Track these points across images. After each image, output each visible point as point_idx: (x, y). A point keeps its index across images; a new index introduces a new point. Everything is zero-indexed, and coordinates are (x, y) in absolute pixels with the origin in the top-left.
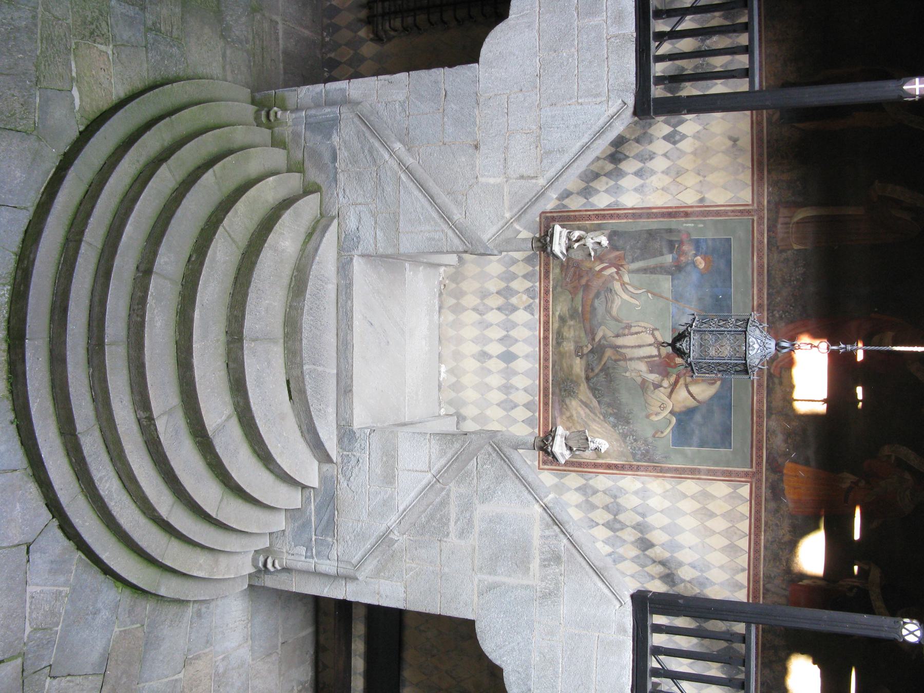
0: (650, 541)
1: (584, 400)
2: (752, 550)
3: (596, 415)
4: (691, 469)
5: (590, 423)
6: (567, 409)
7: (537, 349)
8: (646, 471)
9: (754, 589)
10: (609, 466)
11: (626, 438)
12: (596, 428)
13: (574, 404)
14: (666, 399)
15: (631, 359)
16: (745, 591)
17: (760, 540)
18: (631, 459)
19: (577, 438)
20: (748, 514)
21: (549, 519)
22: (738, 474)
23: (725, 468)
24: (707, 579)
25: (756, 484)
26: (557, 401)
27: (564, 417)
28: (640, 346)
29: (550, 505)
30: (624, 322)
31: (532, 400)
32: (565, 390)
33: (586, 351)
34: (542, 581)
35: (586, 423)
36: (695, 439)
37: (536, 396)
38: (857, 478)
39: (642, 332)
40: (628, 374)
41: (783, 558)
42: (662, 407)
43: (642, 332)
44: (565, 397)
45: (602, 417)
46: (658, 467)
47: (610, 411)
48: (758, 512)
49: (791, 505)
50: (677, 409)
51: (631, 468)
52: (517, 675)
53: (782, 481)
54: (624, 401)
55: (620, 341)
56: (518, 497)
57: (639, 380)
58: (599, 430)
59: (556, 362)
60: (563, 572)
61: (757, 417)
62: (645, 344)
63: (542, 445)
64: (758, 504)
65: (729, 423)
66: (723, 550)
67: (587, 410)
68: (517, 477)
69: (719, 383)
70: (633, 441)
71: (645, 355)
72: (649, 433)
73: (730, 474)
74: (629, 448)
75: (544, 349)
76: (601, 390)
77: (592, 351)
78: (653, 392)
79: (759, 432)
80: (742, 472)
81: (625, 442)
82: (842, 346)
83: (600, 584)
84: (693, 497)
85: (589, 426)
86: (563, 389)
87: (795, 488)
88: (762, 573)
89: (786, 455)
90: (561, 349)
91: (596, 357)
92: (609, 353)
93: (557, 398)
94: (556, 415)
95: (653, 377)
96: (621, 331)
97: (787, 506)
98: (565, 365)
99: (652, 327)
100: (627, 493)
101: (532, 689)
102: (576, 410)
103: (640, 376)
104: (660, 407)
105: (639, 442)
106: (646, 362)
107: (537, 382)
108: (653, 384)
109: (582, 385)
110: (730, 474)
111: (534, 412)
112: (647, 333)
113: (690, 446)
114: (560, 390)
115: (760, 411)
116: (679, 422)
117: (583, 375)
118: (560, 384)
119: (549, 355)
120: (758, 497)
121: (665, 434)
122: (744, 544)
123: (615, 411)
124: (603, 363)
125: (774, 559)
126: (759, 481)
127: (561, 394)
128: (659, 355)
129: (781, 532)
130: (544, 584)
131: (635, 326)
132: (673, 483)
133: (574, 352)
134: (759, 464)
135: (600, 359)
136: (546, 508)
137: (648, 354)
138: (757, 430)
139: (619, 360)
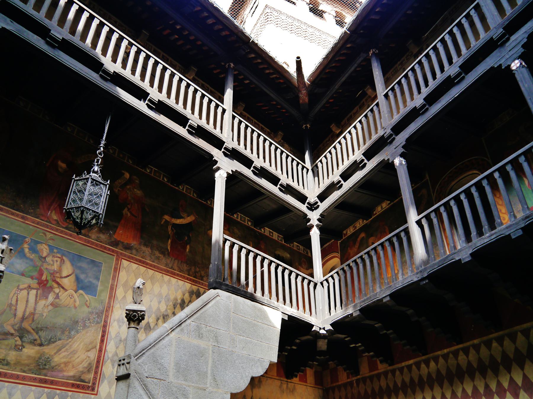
0: (146, 324)
1: (55, 351)
2: (154, 269)
3: (68, 344)
4: (110, 289)
5: (72, 350)
6: (59, 365)
7: (7, 384)
8: (108, 316)
9: (171, 274)
10: (102, 341)
11: (86, 326)
12: (76, 346)
13: (57, 359)
14: (67, 293)
15: (35, 309)
16: (172, 278)
17: (149, 263)
18: (100, 325)
19: (137, 295)
20: (137, 265)
21: (178, 329)
22: (117, 264)
23: (113, 269)
24: (166, 296)
25: (123, 256)
26: (52, 373)
27: (64, 369)
28: (27, 301)
29: (171, 327)
30: (5, 307)
31: (47, 394)
32: (45, 365)
33: (19, 342)
34: (209, 341)
35: (71, 352)
36: (94, 281)
37: (44, 390)
38: (126, 208)
39: (17, 296)
40: (45, 315)
41: (159, 255)
42: (71, 296)
43: (17, 296)
44: (50, 365)
45: (70, 340)
46: (106, 309)
47: (67, 333)
48: (136, 260)
49: (135, 243)
50: (75, 288)
51: (105, 326)
52: (253, 367)
53: (123, 243)
54: (62, 322)
55: (20, 314)
56: (166, 347)
57: (50, 308)
58: (78, 343)
59: (21, 369)
60: (205, 326)
61: (88, 243)
62: (26, 297)
63: (137, 322)
64: (133, 258)
65: (88, 260)
66: (153, 284)
67: (63, 350)
68: (154, 346)
69: (64, 258)
70: (89, 321)
71: (34, 299)
72: (86, 310)
73: (116, 269)
74: (93, 325)
75: (8, 378)
76: (51, 337)
77: (21, 338)
78: (61, 300)
79: (97, 245)
80: (116, 261)
81: (89, 327)
82: (102, 145)
83: (210, 305)
84: (126, 293)
85: (74, 351)
86: (44, 366)
87: (127, 238)
88: (164, 268)
89: (110, 236)
90: (12, 362)
91: (27, 335)
92: (26, 325)
93: (50, 373)
94: (61, 375)
95: (51, 297)
96: (12, 312)
97: (135, 245)
98: (26, 362)
99: (15, 289)
100: (119, 332)
101: (259, 358)
102: (61, 358)
103: (48, 306)
104: (71, 298)
105: (91, 318)
106: (39, 300)
107: (33, 388)
108: (55, 299)
109: (44, 350)
110: (116, 269)
111: (56, 394)
112: (19, 294)
113: (98, 286)
114: (44, 369)
115: (85, 241)
116: (82, 288)
117: (37, 348)
118: (40, 369)
119: (15, 374)
120: (129, 257)
121: (88, 299)
122: (151, 272)
123: (67, 330)
124: (32, 331)
125: (159, 259)
126: (121, 254)
127: (47, 369)
128: (37, 289)
129: (147, 252)
130: (211, 340)
131: (12, 301)
132: (117, 302)
133: (18, 352)
134: (113, 251)
135: (28, 332)
136: (172, 329)
137: (34, 297)
138: (95, 246)
139: (33, 318)
